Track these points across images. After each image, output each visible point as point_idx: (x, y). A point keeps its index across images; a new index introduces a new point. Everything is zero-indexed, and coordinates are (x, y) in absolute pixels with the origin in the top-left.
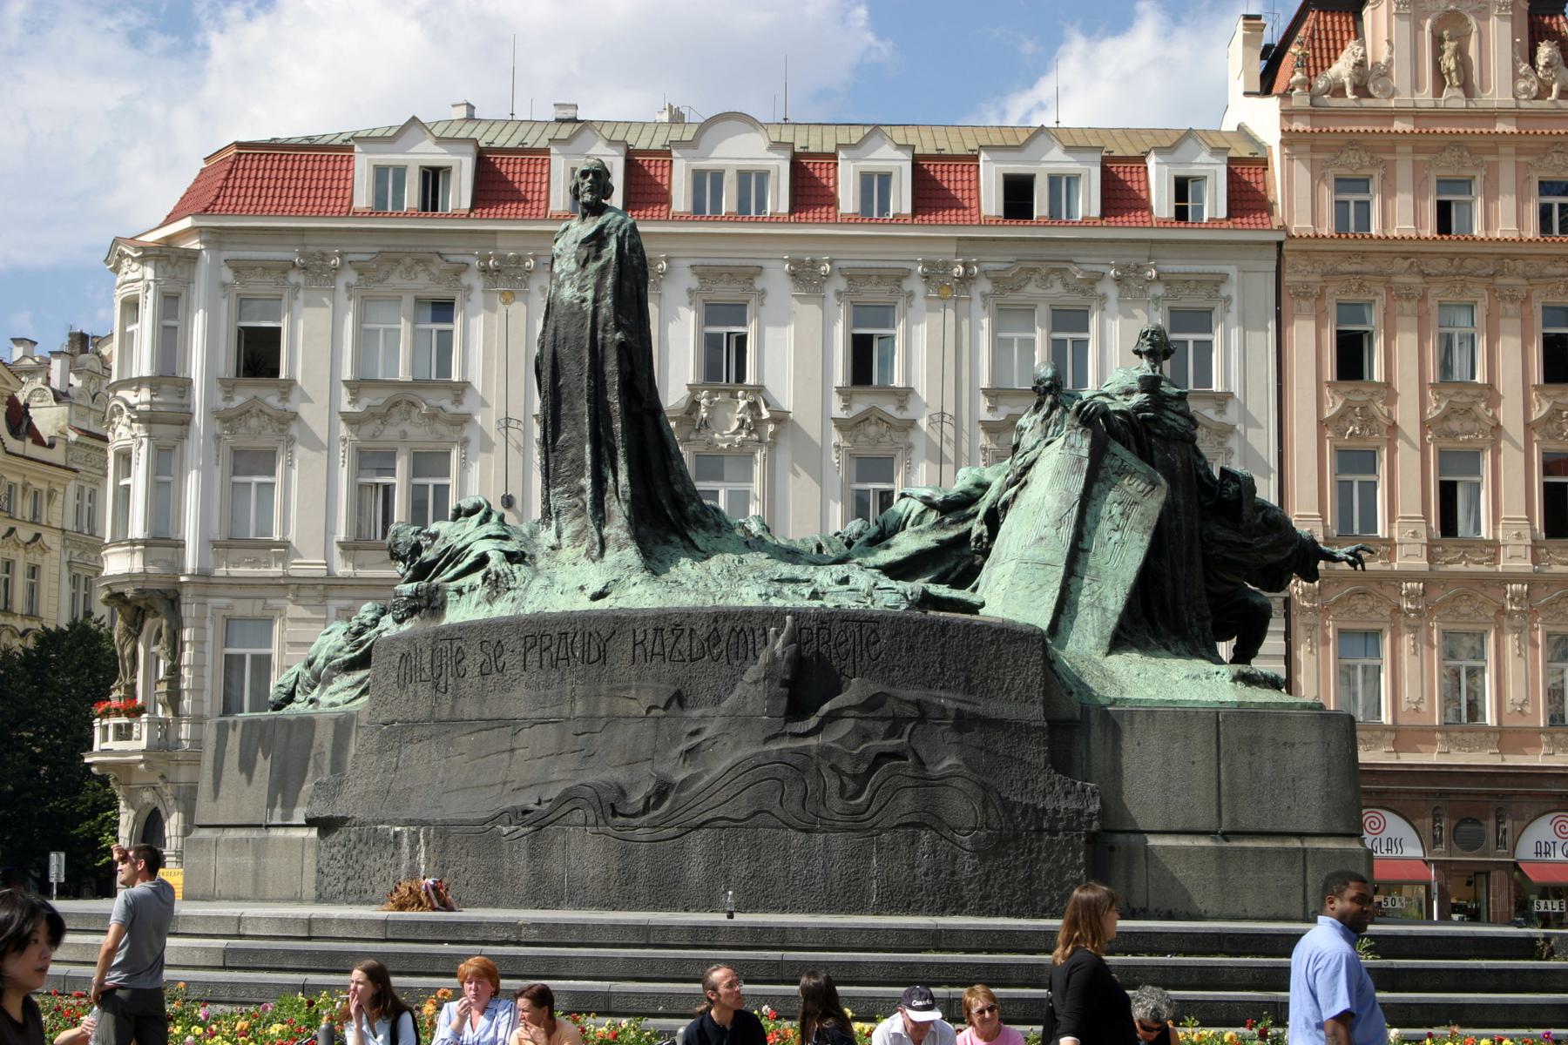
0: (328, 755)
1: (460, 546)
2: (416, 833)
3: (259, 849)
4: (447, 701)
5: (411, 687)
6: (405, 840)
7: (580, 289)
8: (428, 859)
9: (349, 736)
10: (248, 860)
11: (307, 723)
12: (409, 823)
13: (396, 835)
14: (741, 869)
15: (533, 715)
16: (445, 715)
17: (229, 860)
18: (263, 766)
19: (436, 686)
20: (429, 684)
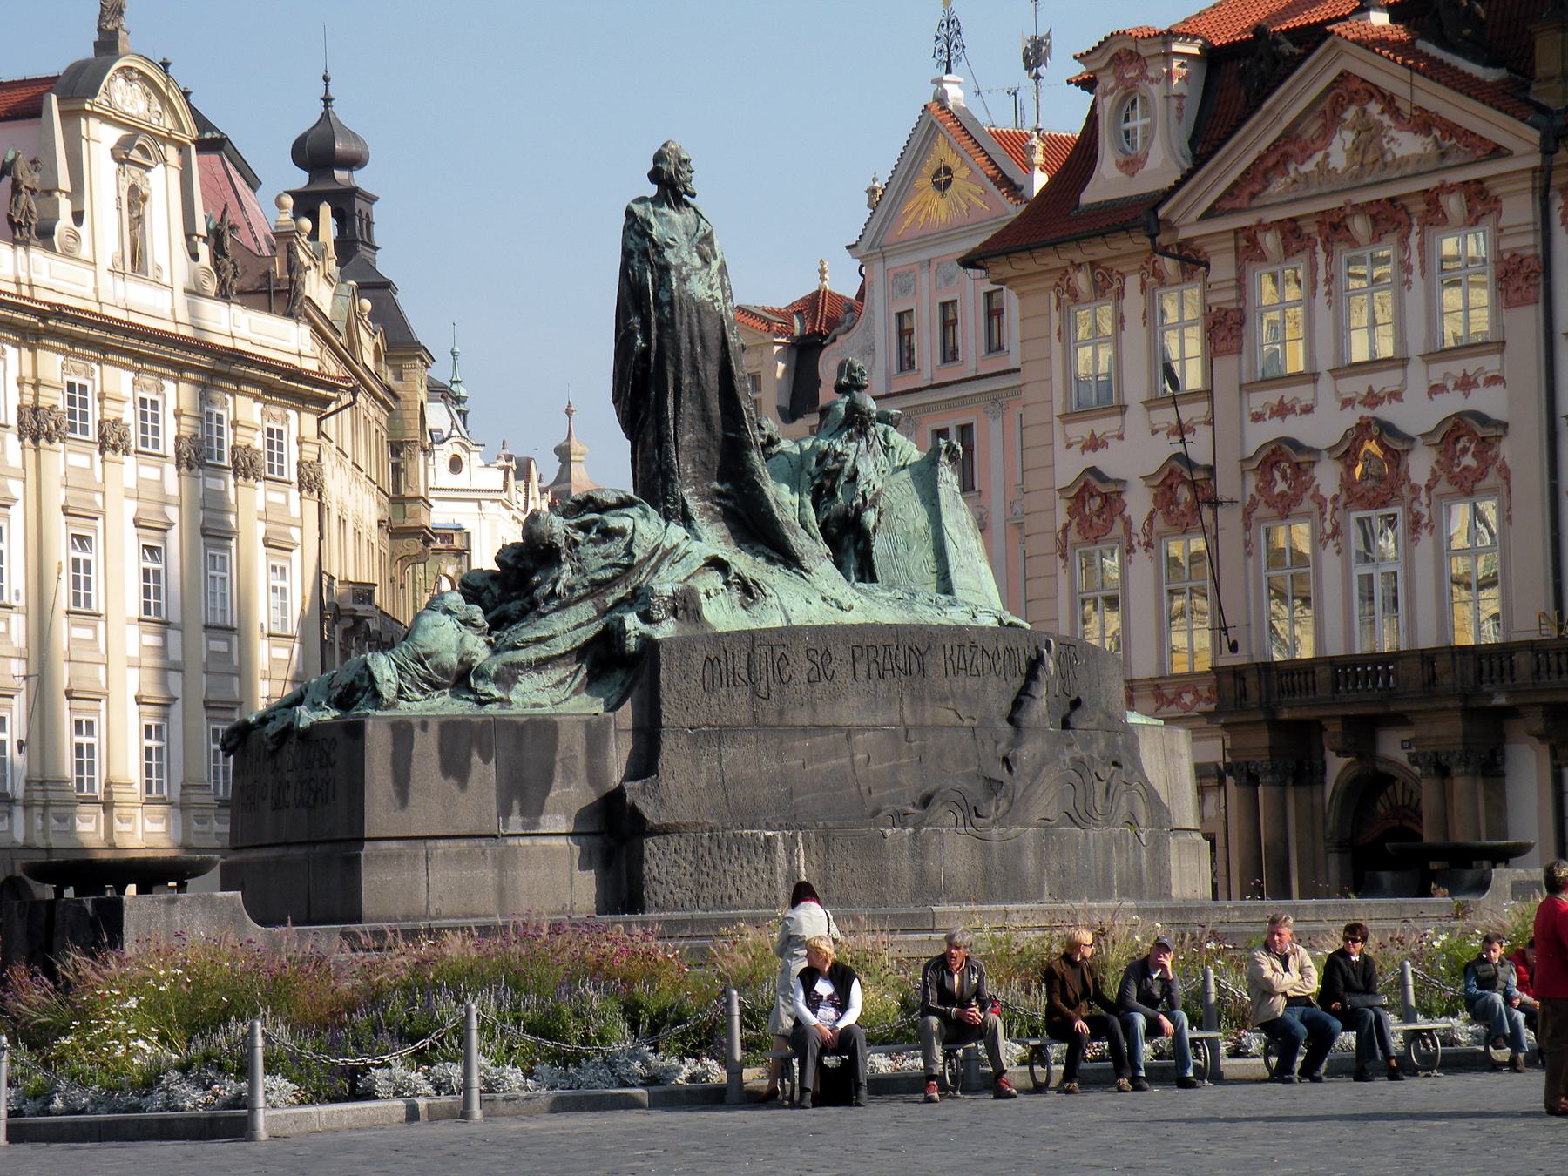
0: (581, 761)
1: (668, 545)
2: (794, 837)
3: (503, 863)
4: (772, 706)
5: (723, 691)
6: (780, 846)
7: (711, 287)
8: (807, 860)
9: (607, 741)
10: (488, 874)
11: (543, 730)
12: (780, 828)
13: (768, 839)
14: (1054, 865)
15: (865, 722)
16: (771, 719)
17: (452, 874)
18: (484, 772)
19: (755, 692)
20: (748, 690)
